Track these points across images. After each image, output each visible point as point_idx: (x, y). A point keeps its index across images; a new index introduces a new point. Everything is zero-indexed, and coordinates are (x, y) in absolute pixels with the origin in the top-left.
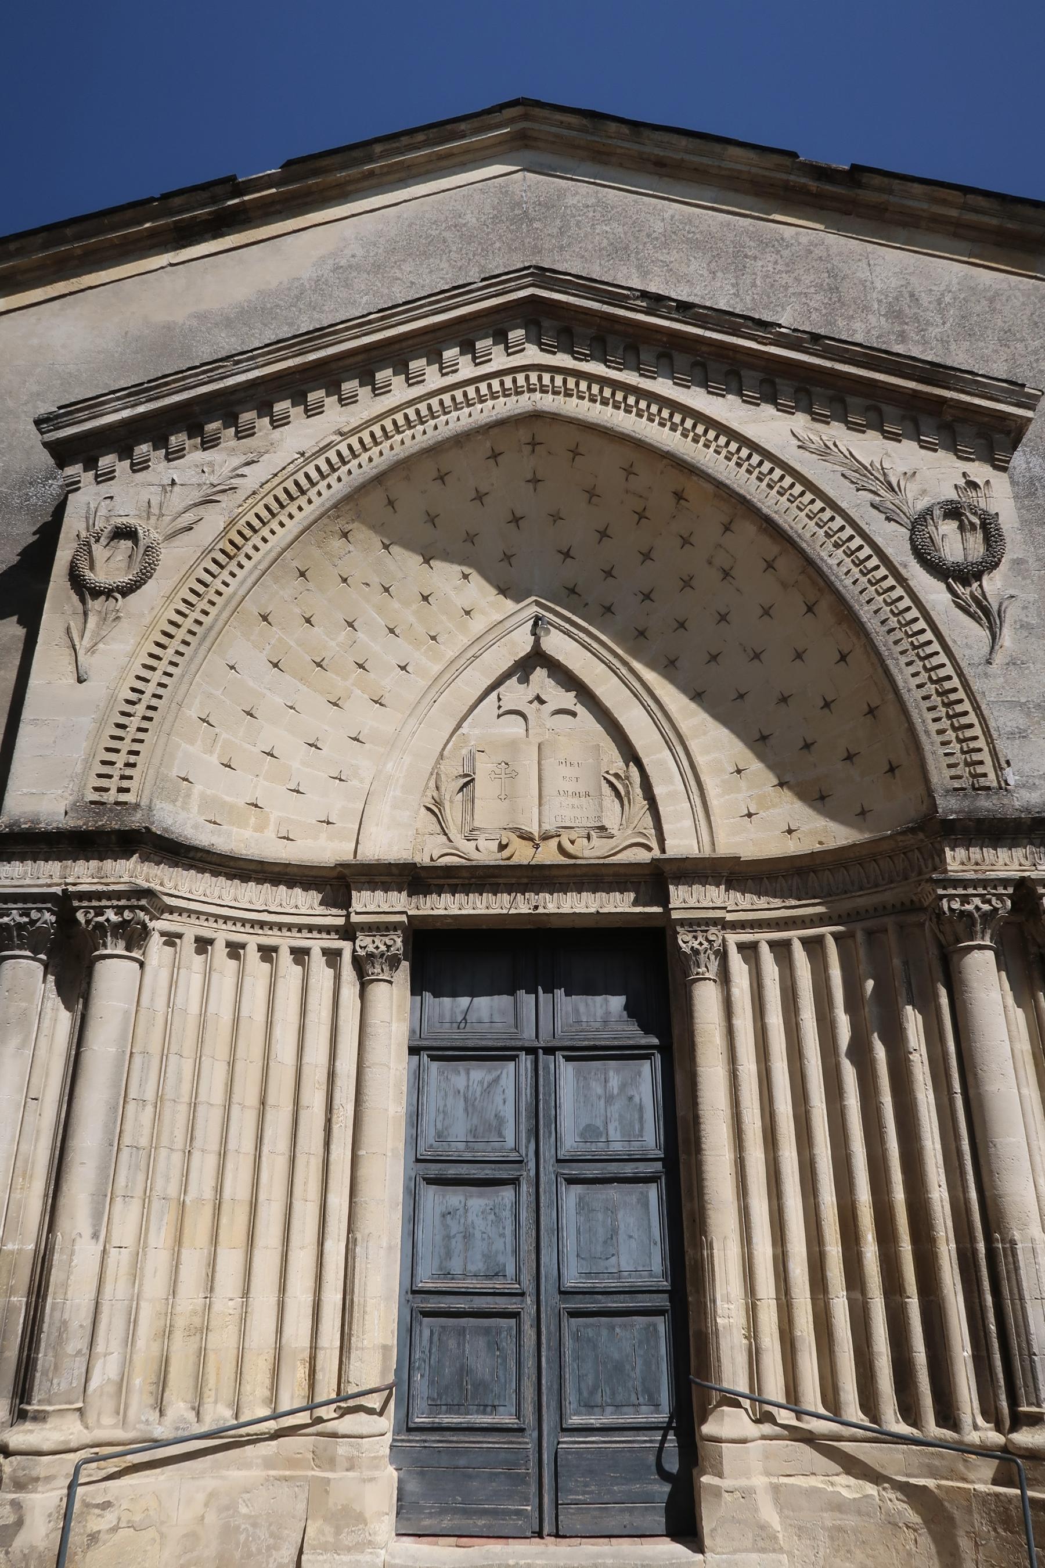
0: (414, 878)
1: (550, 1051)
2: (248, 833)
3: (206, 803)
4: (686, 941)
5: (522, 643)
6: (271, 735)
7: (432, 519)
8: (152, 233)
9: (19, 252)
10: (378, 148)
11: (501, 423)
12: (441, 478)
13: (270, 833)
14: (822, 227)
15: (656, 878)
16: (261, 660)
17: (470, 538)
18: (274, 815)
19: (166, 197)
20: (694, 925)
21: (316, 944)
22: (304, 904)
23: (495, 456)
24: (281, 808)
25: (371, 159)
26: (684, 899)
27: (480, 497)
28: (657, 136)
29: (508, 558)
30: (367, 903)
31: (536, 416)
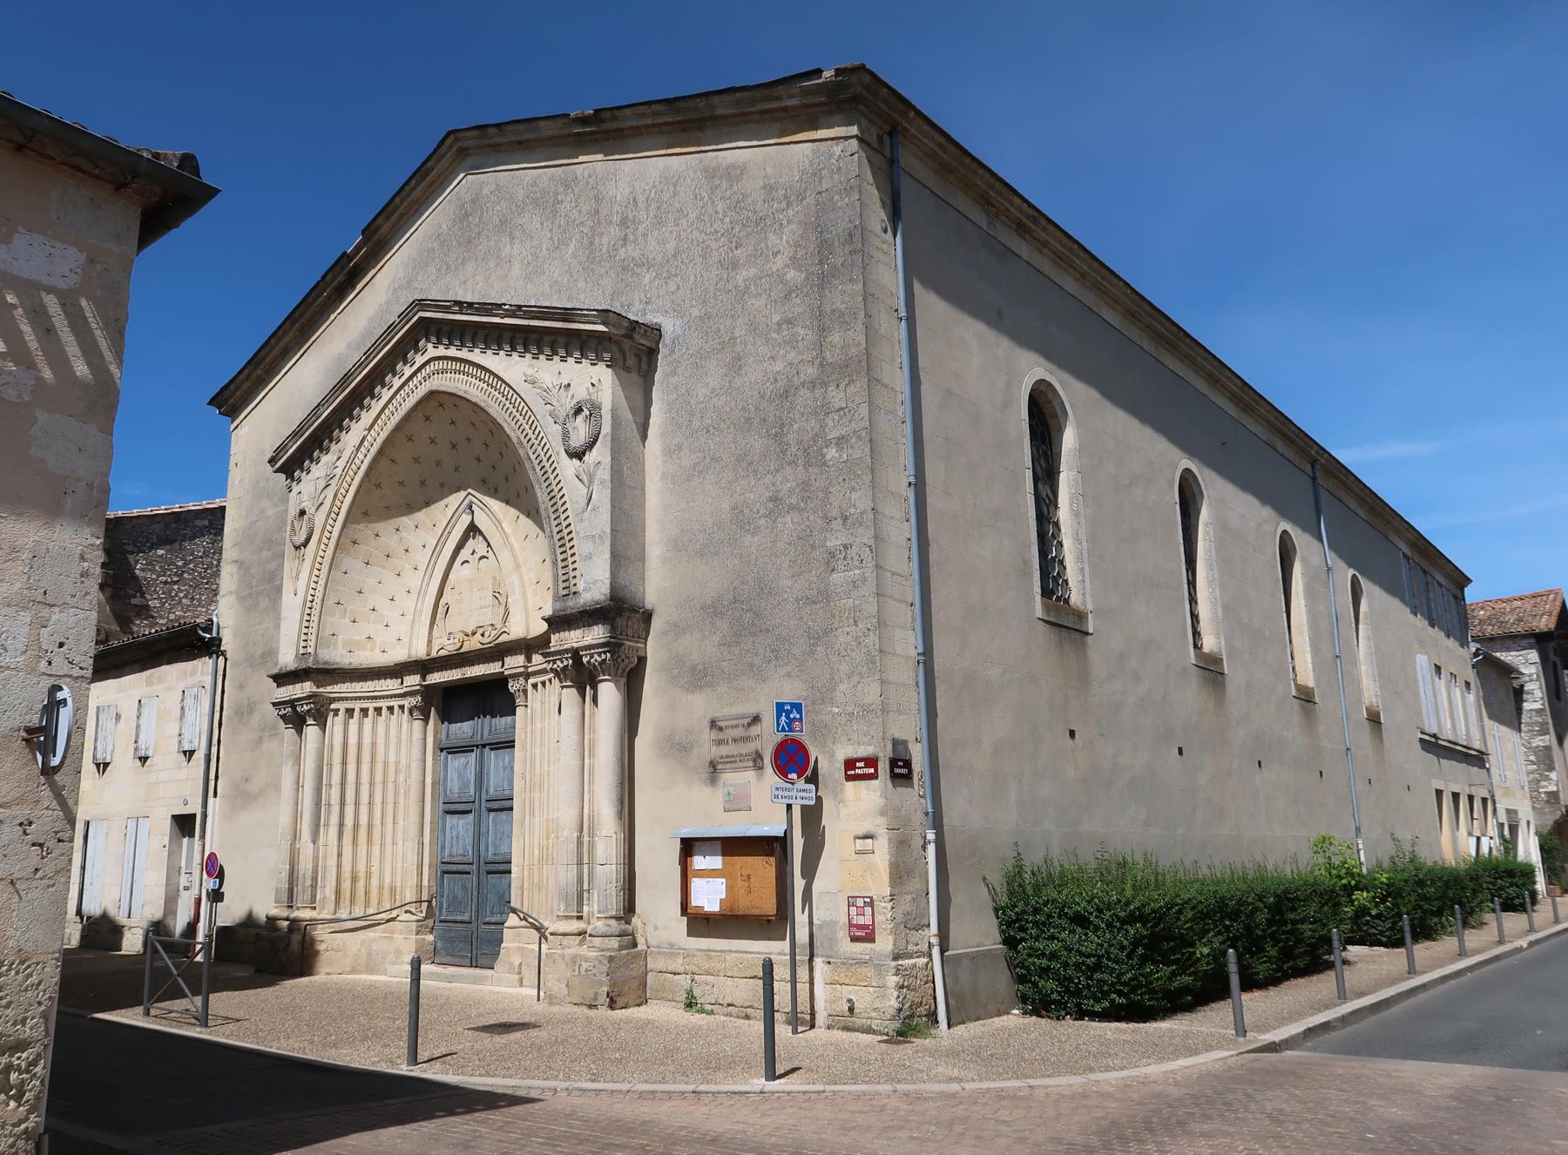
0: (423, 667)
1: (484, 746)
2: (367, 653)
3: (345, 643)
4: (513, 686)
5: (465, 520)
6: (374, 599)
7: (416, 460)
8: (329, 297)
9: (285, 334)
10: (397, 200)
11: (419, 403)
12: (410, 439)
13: (377, 651)
14: (600, 157)
15: (499, 652)
16: (360, 564)
17: (438, 463)
18: (378, 640)
19: (323, 278)
20: (515, 676)
21: (395, 703)
22: (391, 685)
23: (428, 419)
24: (382, 637)
25: (397, 208)
26: (515, 662)
27: (433, 441)
28: (509, 128)
29: (457, 468)
30: (413, 681)
31: (432, 394)
